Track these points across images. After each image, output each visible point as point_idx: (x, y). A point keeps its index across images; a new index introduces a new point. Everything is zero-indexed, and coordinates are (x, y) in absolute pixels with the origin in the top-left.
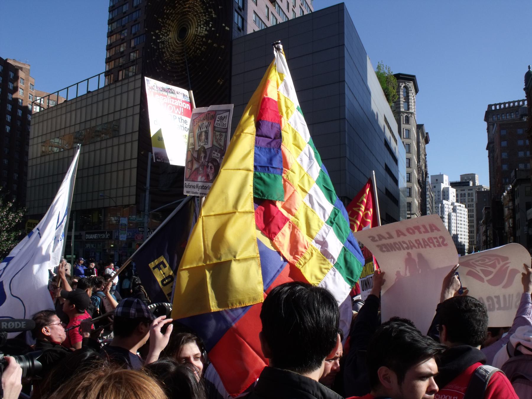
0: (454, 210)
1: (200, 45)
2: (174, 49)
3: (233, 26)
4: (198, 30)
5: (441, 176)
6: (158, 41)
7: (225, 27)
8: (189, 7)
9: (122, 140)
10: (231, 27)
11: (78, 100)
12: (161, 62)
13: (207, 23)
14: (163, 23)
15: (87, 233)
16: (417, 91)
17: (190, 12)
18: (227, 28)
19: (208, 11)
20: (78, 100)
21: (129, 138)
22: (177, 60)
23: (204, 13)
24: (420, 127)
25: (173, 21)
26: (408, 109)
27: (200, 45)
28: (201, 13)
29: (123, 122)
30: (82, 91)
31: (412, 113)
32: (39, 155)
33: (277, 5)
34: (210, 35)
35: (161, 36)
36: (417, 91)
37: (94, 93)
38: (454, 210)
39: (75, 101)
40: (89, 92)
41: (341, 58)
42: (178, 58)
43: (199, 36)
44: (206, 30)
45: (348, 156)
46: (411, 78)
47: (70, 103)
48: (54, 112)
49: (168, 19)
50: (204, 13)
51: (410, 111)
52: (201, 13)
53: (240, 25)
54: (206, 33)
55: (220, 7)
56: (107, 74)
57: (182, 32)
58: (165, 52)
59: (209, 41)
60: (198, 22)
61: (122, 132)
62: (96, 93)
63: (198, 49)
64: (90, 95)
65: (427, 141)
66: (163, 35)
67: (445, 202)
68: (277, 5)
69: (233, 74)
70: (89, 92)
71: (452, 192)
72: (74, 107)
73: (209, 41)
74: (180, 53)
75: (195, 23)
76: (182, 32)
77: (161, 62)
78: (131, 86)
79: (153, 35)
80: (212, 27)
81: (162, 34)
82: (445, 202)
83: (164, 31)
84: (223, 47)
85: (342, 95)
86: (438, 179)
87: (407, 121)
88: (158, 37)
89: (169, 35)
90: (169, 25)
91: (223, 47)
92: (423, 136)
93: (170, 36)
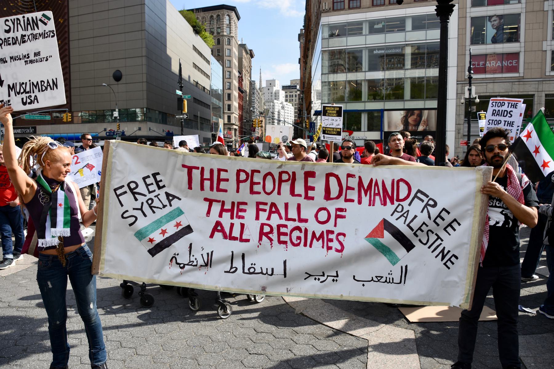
0: (283, 108)
5: (274, 81)
24: (242, 46)
26: (230, 33)
31: (232, 37)
36: (238, 18)
38: (283, 108)
46: (233, 9)
51: (231, 35)
65: (252, 56)
67: (275, 101)
71: (282, 94)
82: (275, 101)
86: (271, 83)
87: (229, 44)
92: (247, 53)
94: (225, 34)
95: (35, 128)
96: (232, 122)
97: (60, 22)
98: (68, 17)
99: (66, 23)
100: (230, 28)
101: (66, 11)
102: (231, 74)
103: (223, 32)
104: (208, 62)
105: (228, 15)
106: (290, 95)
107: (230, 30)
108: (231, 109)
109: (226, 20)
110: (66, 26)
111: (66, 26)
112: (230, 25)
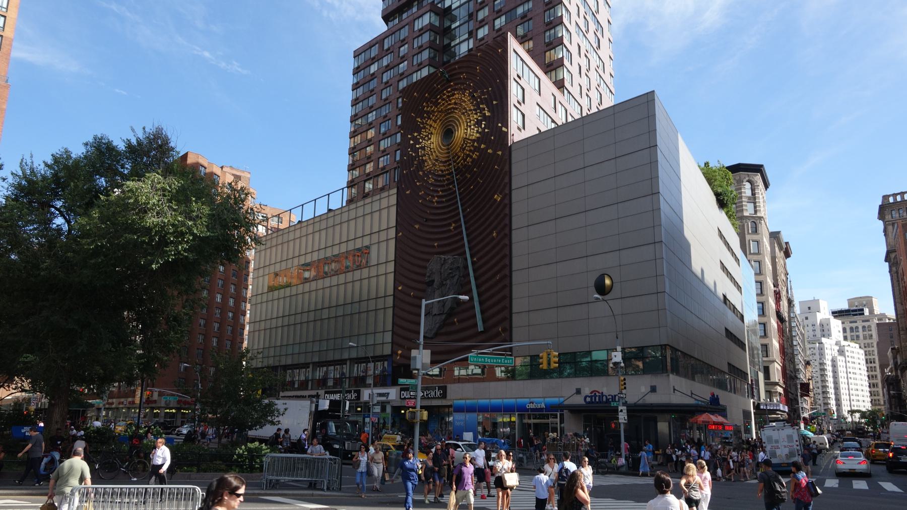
0: (841, 352)
1: (470, 151)
4: (467, 130)
5: (816, 302)
7: (501, 127)
8: (455, 103)
9: (373, 272)
11: (317, 220)
12: (421, 173)
13: (478, 123)
14: (423, 123)
15: (326, 393)
16: (766, 186)
17: (456, 109)
19: (479, 108)
20: (317, 220)
21: (382, 269)
22: (442, 171)
23: (475, 110)
24: (775, 236)
25: (435, 121)
26: (756, 212)
27: (470, 151)
28: (470, 110)
29: (374, 250)
30: (322, 210)
31: (761, 218)
32: (266, 290)
33: (566, 91)
36: (766, 186)
37: (337, 212)
38: (841, 352)
39: (312, 222)
40: (330, 210)
41: (653, 163)
42: (443, 168)
44: (477, 131)
45: (667, 290)
46: (757, 169)
47: (305, 224)
48: (286, 236)
49: (429, 118)
50: (475, 110)
51: (759, 215)
52: (470, 110)
53: (520, 124)
54: (478, 135)
55: (494, 102)
56: (351, 184)
57: (448, 133)
59: (483, 146)
61: (374, 261)
62: (339, 212)
63: (468, 156)
64: (331, 214)
65: (787, 254)
67: (824, 340)
68: (566, 91)
69: (513, 187)
70: (330, 210)
71: (836, 325)
72: (310, 230)
73: (483, 146)
74: (446, 162)
76: (448, 133)
77: (421, 173)
78: (384, 203)
79: (410, 139)
80: (485, 128)
81: (422, 138)
82: (824, 340)
84: (500, 153)
85: (656, 210)
86: (811, 307)
87: (756, 231)
90: (431, 126)
91: (500, 153)
92: (781, 248)
94: (746, 214)
95: (444, 389)
96: (772, 380)
97: (496, 200)
98: (510, 190)
99: (506, 201)
100: (755, 203)
101: (507, 180)
102: (764, 286)
103: (742, 210)
104: (737, 260)
105: (749, 181)
106: (864, 327)
107: (755, 207)
108: (770, 353)
109: (747, 190)
110: (506, 205)
111: (506, 205)
112: (755, 199)
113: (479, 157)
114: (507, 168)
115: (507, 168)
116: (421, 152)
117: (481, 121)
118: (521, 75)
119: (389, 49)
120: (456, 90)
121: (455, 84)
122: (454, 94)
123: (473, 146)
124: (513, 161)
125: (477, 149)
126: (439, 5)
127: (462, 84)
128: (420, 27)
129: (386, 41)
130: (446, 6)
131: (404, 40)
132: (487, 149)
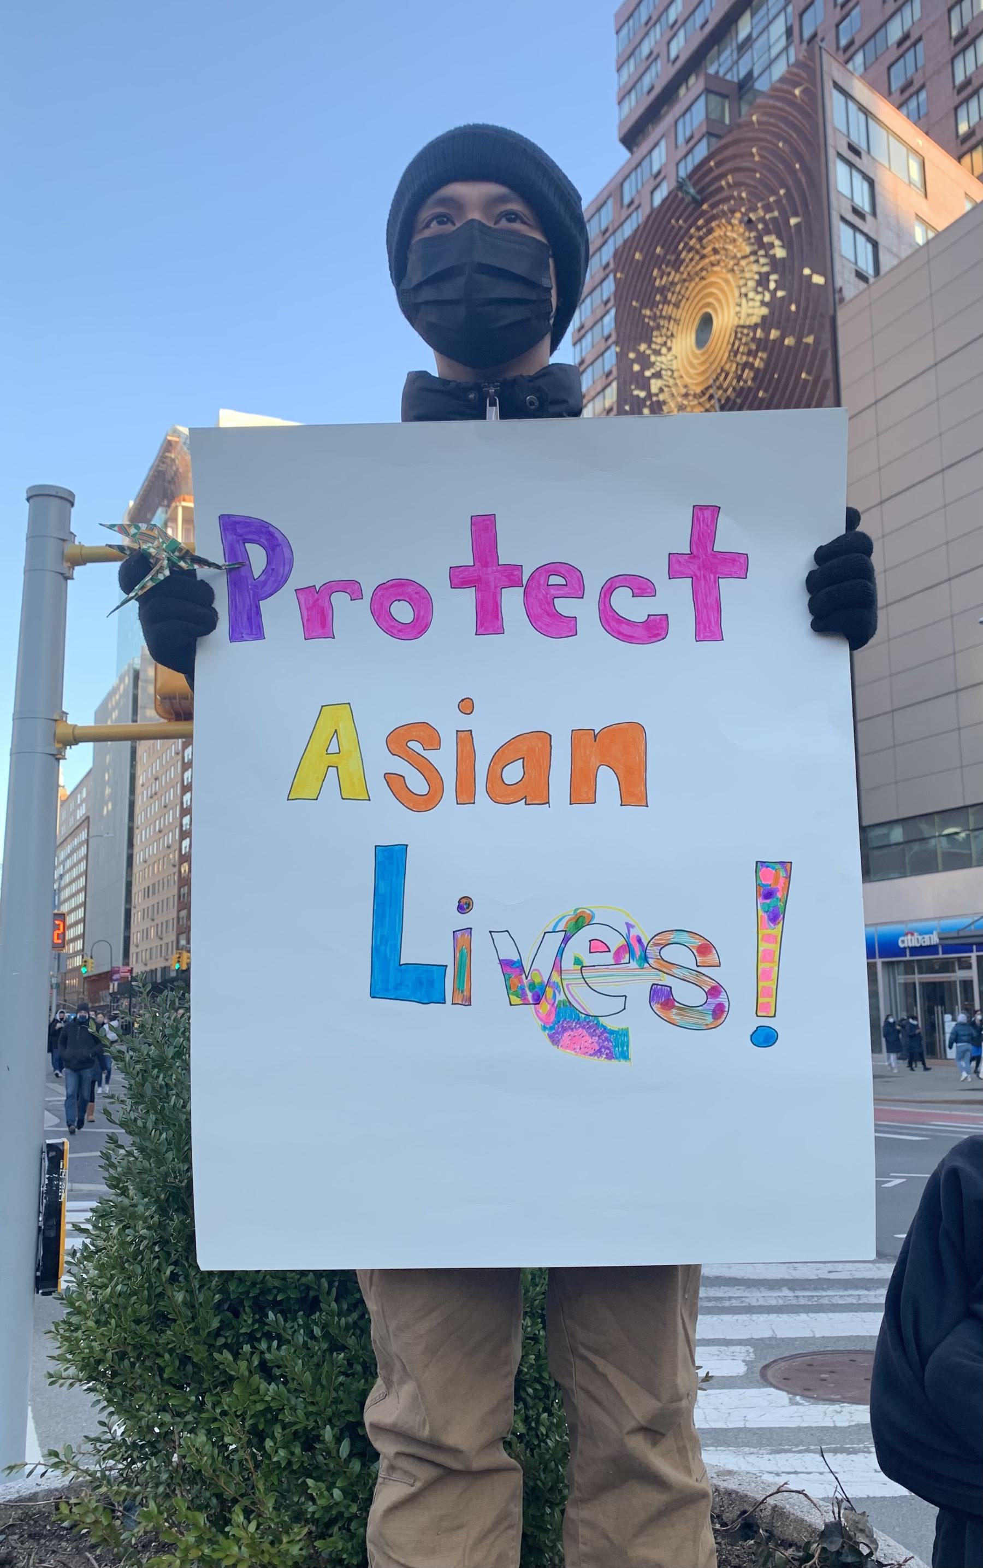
1: (750, 353)
2: (686, 386)
3: (837, 267)
6: (648, 374)
7: (810, 277)
10: (830, 274)
14: (654, 318)
18: (818, 280)
19: (761, 245)
23: (754, 253)
34: (776, 315)
35: (653, 358)
43: (743, 327)
44: (763, 303)
54: (765, 311)
58: (664, 403)
59: (774, 334)
60: (740, 287)
66: (657, 353)
73: (774, 334)
75: (732, 291)
79: (633, 361)
80: (776, 290)
83: (659, 340)
88: (645, 362)
89: (669, 349)
90: (670, 318)
91: (810, 340)
93: (674, 351)
113: (767, 362)
114: (828, 372)
115: (828, 372)
116: (655, 385)
117: (768, 274)
118: (863, 146)
119: (632, 202)
120: (714, 218)
121: (713, 206)
122: (710, 231)
123: (753, 339)
124: (841, 352)
125: (762, 344)
126: (728, 77)
127: (726, 200)
128: (688, 134)
129: (626, 186)
130: (743, 73)
131: (659, 173)
132: (783, 337)
